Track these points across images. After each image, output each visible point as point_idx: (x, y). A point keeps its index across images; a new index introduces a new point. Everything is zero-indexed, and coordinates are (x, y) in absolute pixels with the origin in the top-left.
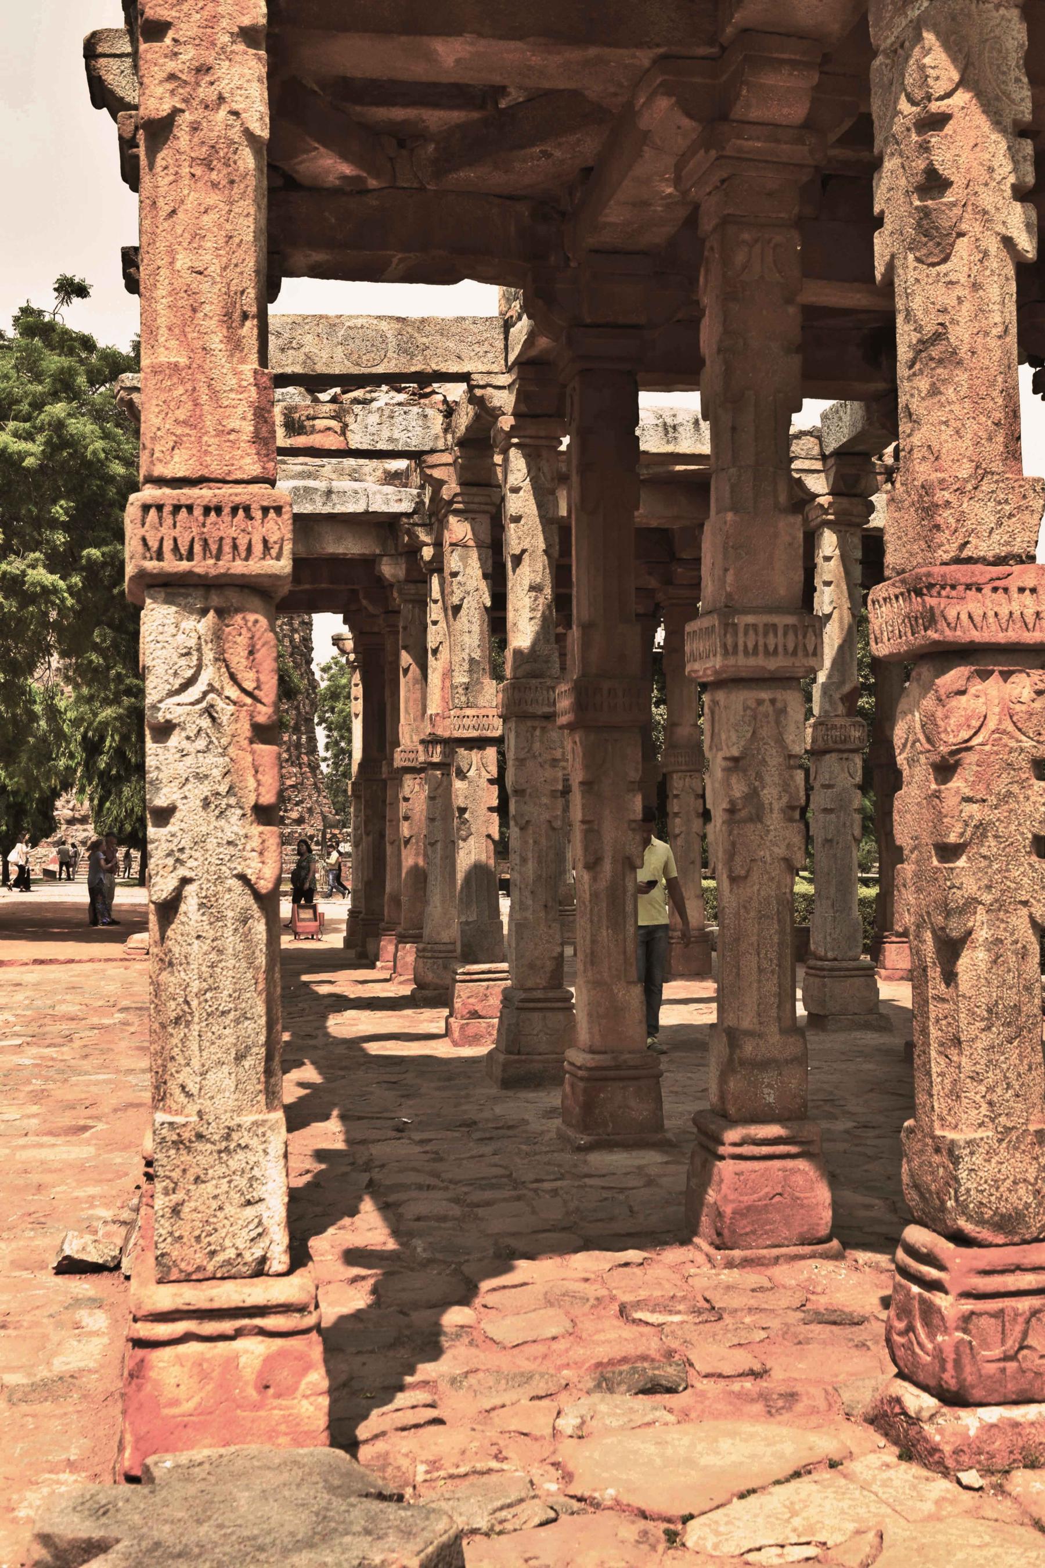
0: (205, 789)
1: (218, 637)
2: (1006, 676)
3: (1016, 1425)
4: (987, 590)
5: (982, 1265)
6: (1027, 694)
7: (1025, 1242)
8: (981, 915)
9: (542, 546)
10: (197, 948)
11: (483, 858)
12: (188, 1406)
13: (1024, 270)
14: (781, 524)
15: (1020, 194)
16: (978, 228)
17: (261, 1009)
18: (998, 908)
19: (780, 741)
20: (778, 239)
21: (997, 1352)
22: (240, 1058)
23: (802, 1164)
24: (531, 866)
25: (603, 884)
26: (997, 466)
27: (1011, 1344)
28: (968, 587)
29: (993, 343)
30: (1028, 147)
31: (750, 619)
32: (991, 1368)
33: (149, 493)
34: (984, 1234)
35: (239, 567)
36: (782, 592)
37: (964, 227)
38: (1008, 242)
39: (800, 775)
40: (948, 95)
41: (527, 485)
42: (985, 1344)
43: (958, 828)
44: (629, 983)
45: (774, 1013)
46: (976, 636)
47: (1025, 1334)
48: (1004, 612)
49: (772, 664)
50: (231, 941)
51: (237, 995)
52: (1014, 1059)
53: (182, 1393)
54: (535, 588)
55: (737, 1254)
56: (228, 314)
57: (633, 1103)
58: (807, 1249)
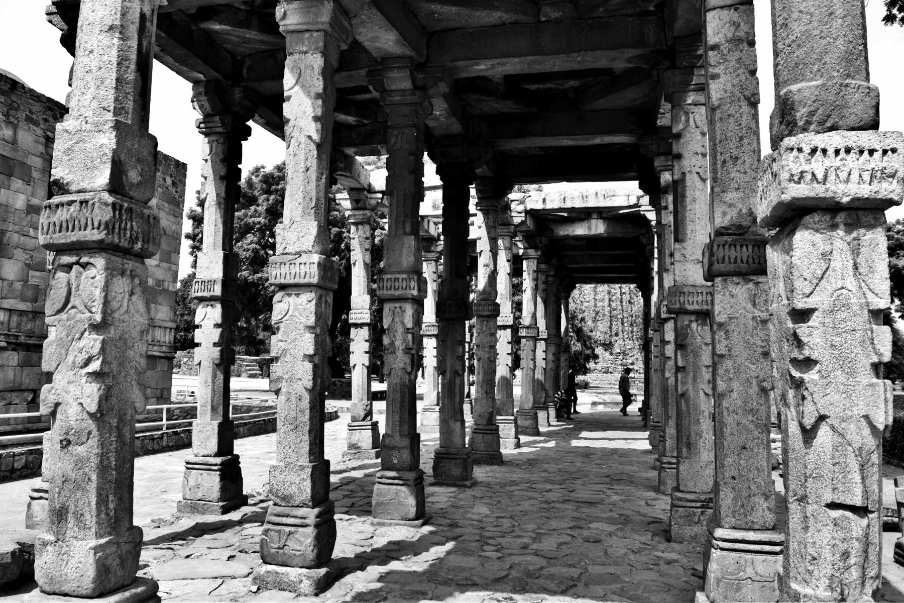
2: (297, 295)
3: (277, 573)
4: (288, 264)
5: (275, 512)
6: (305, 302)
7: (293, 506)
8: (284, 383)
9: (489, 249)
11: (504, 374)
12: (39, 519)
13: (319, 146)
14: (406, 240)
15: (316, 119)
16: (298, 134)
19: (403, 323)
20: (407, 131)
21: (276, 546)
23: (404, 488)
24: (480, 375)
25: (446, 381)
26: (299, 219)
27: (282, 544)
28: (281, 263)
29: (301, 175)
30: (320, 102)
31: (389, 276)
32: (273, 551)
34: (278, 501)
36: (405, 265)
37: (293, 134)
38: (310, 137)
39: (410, 336)
40: (292, 88)
41: (483, 225)
42: (272, 541)
43: (276, 351)
44: (455, 420)
45: (397, 428)
46: (283, 281)
47: (286, 540)
48: (293, 272)
49: (397, 293)
52: (293, 438)
53: (38, 514)
54: (486, 265)
55: (376, 520)
57: (453, 468)
58: (404, 522)
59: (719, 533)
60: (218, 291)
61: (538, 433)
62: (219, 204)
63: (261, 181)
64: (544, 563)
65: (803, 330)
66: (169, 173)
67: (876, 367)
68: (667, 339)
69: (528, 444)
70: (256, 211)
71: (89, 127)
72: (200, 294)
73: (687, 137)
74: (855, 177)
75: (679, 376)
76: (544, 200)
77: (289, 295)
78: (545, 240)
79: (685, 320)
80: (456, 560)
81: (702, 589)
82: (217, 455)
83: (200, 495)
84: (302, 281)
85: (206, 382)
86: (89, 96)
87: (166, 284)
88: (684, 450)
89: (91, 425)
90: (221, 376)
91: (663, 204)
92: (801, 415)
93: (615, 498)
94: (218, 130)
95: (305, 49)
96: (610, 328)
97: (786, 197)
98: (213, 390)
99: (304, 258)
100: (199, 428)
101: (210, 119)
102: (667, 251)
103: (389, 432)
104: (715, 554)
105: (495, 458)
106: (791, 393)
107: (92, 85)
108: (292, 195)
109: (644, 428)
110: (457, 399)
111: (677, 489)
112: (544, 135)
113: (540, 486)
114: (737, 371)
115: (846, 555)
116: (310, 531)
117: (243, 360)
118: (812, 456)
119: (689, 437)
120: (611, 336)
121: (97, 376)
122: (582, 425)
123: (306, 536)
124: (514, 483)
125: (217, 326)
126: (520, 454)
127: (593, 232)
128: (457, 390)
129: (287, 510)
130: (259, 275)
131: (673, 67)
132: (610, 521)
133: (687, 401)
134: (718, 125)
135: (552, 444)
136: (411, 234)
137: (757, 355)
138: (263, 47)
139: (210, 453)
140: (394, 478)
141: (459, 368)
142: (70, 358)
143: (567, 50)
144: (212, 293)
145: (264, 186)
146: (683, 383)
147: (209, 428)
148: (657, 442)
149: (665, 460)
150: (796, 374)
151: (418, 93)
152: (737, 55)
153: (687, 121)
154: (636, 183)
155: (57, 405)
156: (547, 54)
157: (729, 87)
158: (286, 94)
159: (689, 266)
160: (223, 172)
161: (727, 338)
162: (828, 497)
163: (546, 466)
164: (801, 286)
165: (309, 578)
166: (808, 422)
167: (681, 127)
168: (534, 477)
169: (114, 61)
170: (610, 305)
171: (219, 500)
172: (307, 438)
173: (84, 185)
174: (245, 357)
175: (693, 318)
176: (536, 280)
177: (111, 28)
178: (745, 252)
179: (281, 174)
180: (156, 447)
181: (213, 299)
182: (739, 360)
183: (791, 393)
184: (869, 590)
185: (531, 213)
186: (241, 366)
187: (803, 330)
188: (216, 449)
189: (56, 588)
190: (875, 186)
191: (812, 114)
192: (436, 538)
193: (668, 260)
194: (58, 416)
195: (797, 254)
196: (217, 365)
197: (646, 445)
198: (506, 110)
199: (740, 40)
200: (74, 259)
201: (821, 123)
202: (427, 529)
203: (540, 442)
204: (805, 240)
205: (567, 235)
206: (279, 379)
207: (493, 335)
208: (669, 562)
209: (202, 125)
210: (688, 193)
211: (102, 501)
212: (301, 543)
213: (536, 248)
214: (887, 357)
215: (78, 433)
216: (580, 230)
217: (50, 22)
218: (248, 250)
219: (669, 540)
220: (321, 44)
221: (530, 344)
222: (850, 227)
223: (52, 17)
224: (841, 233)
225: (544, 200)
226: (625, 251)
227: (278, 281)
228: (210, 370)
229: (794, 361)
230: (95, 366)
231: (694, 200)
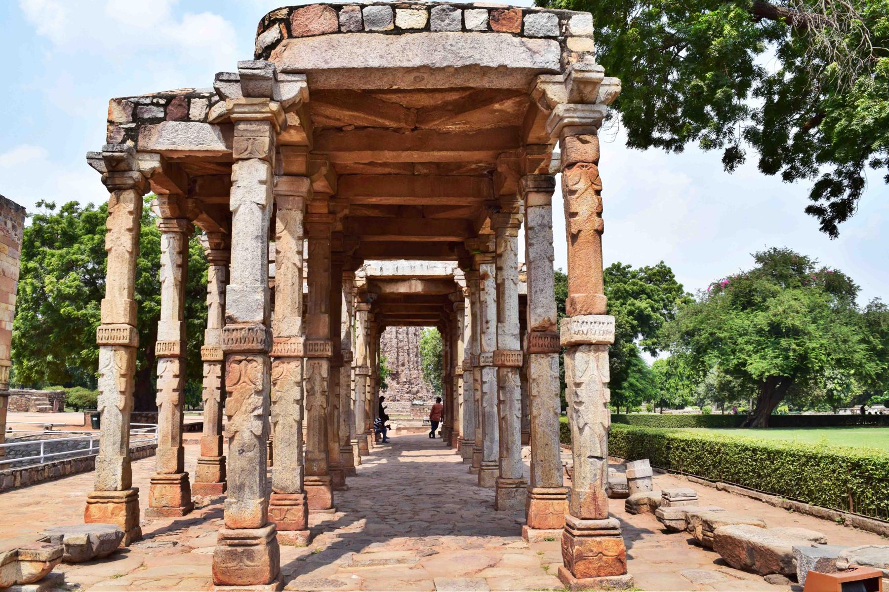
0: (109, 388)
1: (114, 356)
2: (289, 363)
10: (106, 421)
17: (120, 434)
18: (285, 416)
19: (320, 374)
22: (114, 444)
23: (323, 487)
26: (289, 315)
27: (282, 517)
29: (289, 288)
33: (102, 326)
35: (118, 342)
36: (321, 334)
38: (294, 264)
39: (325, 383)
42: (276, 516)
46: (279, 354)
49: (316, 354)
50: (113, 419)
51: (114, 431)
56: (120, 289)
59: (535, 490)
60: (177, 350)
61: (368, 454)
62: (176, 285)
63: (83, 221)
64: (427, 524)
65: (579, 390)
66: (10, 216)
67: (605, 404)
68: (484, 380)
69: (368, 461)
70: (79, 249)
71: (248, 289)
72: (161, 353)
73: (505, 256)
74: (597, 333)
75: (501, 406)
76: (381, 269)
77: (283, 363)
78: (374, 296)
79: (504, 371)
80: (373, 526)
81: (526, 524)
82: (177, 472)
83: (164, 503)
84: (293, 354)
85: (167, 418)
86: (247, 273)
87: (4, 323)
88: (505, 453)
89: (256, 441)
90: (178, 414)
91: (482, 287)
92: (578, 423)
93: (452, 491)
94: (175, 230)
95: (290, 207)
96: (397, 358)
97: (573, 340)
98: (173, 424)
99: (293, 340)
100: (161, 453)
101: (169, 221)
102: (484, 320)
103: (310, 449)
104: (533, 502)
105: (352, 472)
106: (574, 415)
107: (249, 267)
108: (284, 300)
109: (450, 446)
110: (336, 426)
111: (501, 477)
112: (400, 233)
113: (396, 487)
114: (543, 404)
115: (595, 475)
116: (301, 507)
117: (31, 394)
118: (582, 439)
119: (507, 444)
120: (398, 366)
121: (259, 417)
122: (398, 446)
123: (299, 511)
124: (375, 487)
125: (176, 376)
126: (365, 468)
127: (413, 291)
128: (336, 420)
129: (284, 496)
130: (84, 311)
131: (498, 212)
132: (454, 503)
133: (506, 423)
134: (533, 271)
135: (384, 461)
136: (326, 312)
137: (553, 395)
138: (214, 173)
139: (171, 471)
140: (316, 481)
141: (336, 403)
142: (243, 409)
143: (432, 195)
144: (172, 352)
145: (87, 226)
146: (504, 411)
147: (170, 452)
148: (474, 453)
149: (484, 464)
150: (576, 407)
151: (331, 216)
152: (543, 233)
153: (506, 246)
154: (457, 262)
155: (236, 432)
156: (417, 197)
157: (539, 251)
158: (277, 235)
159: (507, 337)
160: (179, 262)
161: (538, 387)
162: (589, 454)
163: (390, 476)
164: (578, 374)
165: (302, 536)
166: (581, 426)
167: (502, 250)
168: (387, 482)
169: (260, 254)
170: (397, 337)
171: (180, 505)
172: (296, 451)
173: (248, 319)
174: (34, 391)
175: (509, 370)
176: (365, 328)
177: (257, 237)
178: (547, 341)
179: (105, 215)
180: (40, 478)
181: (173, 356)
182: (544, 398)
183: (574, 415)
184: (604, 488)
185: (371, 280)
186: (29, 400)
187: (579, 390)
188: (176, 468)
189: (239, 526)
190: (604, 337)
191: (582, 307)
192: (352, 518)
193: (485, 326)
194: (236, 438)
195: (577, 361)
196: (176, 406)
197: (459, 459)
198: (373, 215)
199: (545, 226)
200: (244, 358)
201: (586, 310)
202: (341, 514)
203: (374, 460)
204: (578, 355)
205: (393, 293)
206: (278, 415)
207: (349, 376)
208: (501, 519)
209: (162, 226)
210: (506, 292)
211: (261, 480)
212: (295, 515)
213: (367, 302)
214: (609, 400)
215: (249, 446)
216: (403, 289)
217: (91, 164)
218: (71, 287)
219: (496, 510)
220: (301, 205)
221: (363, 380)
222: (596, 350)
223: (92, 161)
224: (592, 353)
225: (381, 269)
226: (438, 306)
227: (276, 354)
228: (171, 409)
229: (575, 402)
230: (260, 411)
231: (510, 296)
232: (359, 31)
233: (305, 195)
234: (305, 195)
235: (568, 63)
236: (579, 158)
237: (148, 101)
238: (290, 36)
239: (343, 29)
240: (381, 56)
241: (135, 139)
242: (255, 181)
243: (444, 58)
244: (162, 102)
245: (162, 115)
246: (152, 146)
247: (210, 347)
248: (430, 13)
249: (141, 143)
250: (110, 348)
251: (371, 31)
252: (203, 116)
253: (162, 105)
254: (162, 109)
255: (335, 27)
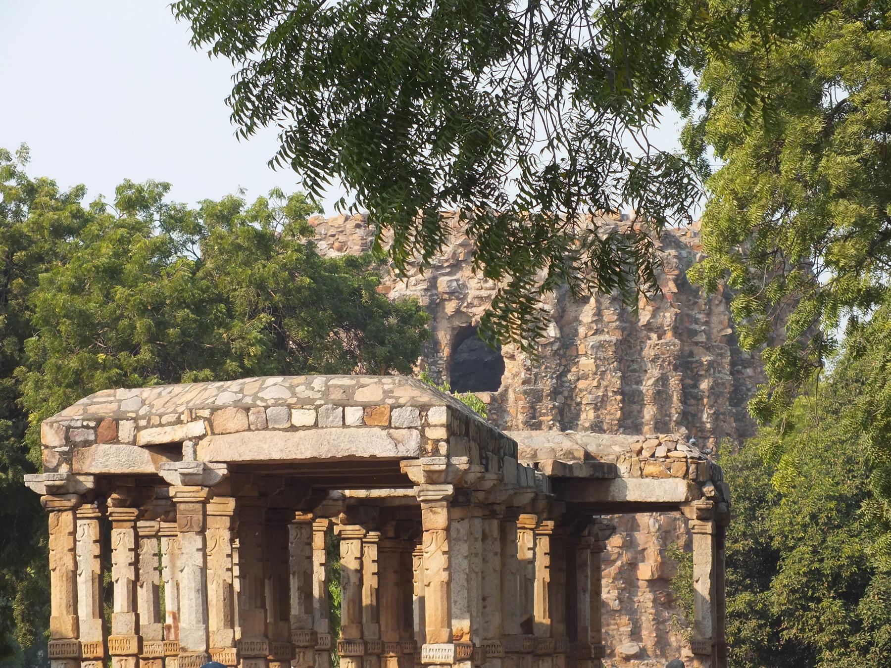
35: (69, 656)
144: (95, 655)
232: (263, 429)
233: (232, 514)
234: (232, 514)
235: (425, 449)
236: (432, 527)
237: (79, 424)
238: (213, 433)
239: (252, 427)
240: (281, 451)
241: (69, 461)
242: (195, 550)
243: (329, 451)
244: (92, 424)
245: (92, 437)
246: (86, 469)
247: (120, 637)
248: (317, 412)
249: (76, 466)
250: (61, 662)
251: (274, 429)
252: (132, 438)
253: (92, 428)
254: (92, 431)
255: (246, 426)
